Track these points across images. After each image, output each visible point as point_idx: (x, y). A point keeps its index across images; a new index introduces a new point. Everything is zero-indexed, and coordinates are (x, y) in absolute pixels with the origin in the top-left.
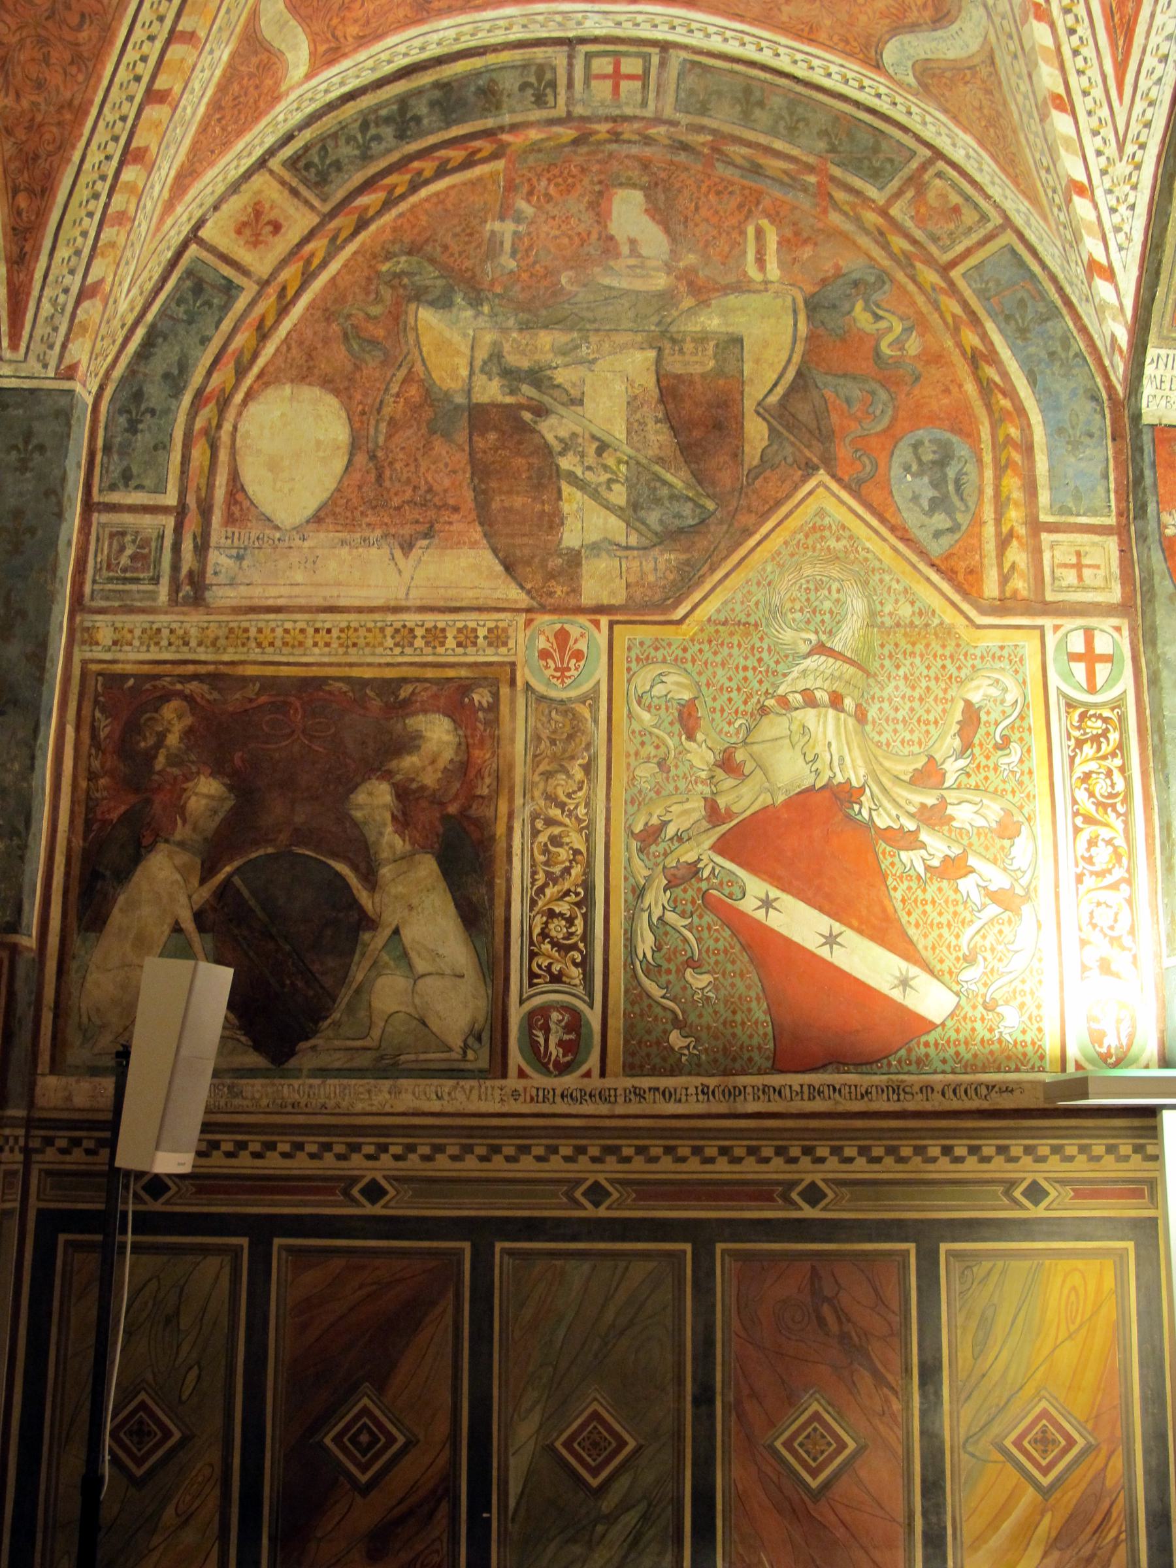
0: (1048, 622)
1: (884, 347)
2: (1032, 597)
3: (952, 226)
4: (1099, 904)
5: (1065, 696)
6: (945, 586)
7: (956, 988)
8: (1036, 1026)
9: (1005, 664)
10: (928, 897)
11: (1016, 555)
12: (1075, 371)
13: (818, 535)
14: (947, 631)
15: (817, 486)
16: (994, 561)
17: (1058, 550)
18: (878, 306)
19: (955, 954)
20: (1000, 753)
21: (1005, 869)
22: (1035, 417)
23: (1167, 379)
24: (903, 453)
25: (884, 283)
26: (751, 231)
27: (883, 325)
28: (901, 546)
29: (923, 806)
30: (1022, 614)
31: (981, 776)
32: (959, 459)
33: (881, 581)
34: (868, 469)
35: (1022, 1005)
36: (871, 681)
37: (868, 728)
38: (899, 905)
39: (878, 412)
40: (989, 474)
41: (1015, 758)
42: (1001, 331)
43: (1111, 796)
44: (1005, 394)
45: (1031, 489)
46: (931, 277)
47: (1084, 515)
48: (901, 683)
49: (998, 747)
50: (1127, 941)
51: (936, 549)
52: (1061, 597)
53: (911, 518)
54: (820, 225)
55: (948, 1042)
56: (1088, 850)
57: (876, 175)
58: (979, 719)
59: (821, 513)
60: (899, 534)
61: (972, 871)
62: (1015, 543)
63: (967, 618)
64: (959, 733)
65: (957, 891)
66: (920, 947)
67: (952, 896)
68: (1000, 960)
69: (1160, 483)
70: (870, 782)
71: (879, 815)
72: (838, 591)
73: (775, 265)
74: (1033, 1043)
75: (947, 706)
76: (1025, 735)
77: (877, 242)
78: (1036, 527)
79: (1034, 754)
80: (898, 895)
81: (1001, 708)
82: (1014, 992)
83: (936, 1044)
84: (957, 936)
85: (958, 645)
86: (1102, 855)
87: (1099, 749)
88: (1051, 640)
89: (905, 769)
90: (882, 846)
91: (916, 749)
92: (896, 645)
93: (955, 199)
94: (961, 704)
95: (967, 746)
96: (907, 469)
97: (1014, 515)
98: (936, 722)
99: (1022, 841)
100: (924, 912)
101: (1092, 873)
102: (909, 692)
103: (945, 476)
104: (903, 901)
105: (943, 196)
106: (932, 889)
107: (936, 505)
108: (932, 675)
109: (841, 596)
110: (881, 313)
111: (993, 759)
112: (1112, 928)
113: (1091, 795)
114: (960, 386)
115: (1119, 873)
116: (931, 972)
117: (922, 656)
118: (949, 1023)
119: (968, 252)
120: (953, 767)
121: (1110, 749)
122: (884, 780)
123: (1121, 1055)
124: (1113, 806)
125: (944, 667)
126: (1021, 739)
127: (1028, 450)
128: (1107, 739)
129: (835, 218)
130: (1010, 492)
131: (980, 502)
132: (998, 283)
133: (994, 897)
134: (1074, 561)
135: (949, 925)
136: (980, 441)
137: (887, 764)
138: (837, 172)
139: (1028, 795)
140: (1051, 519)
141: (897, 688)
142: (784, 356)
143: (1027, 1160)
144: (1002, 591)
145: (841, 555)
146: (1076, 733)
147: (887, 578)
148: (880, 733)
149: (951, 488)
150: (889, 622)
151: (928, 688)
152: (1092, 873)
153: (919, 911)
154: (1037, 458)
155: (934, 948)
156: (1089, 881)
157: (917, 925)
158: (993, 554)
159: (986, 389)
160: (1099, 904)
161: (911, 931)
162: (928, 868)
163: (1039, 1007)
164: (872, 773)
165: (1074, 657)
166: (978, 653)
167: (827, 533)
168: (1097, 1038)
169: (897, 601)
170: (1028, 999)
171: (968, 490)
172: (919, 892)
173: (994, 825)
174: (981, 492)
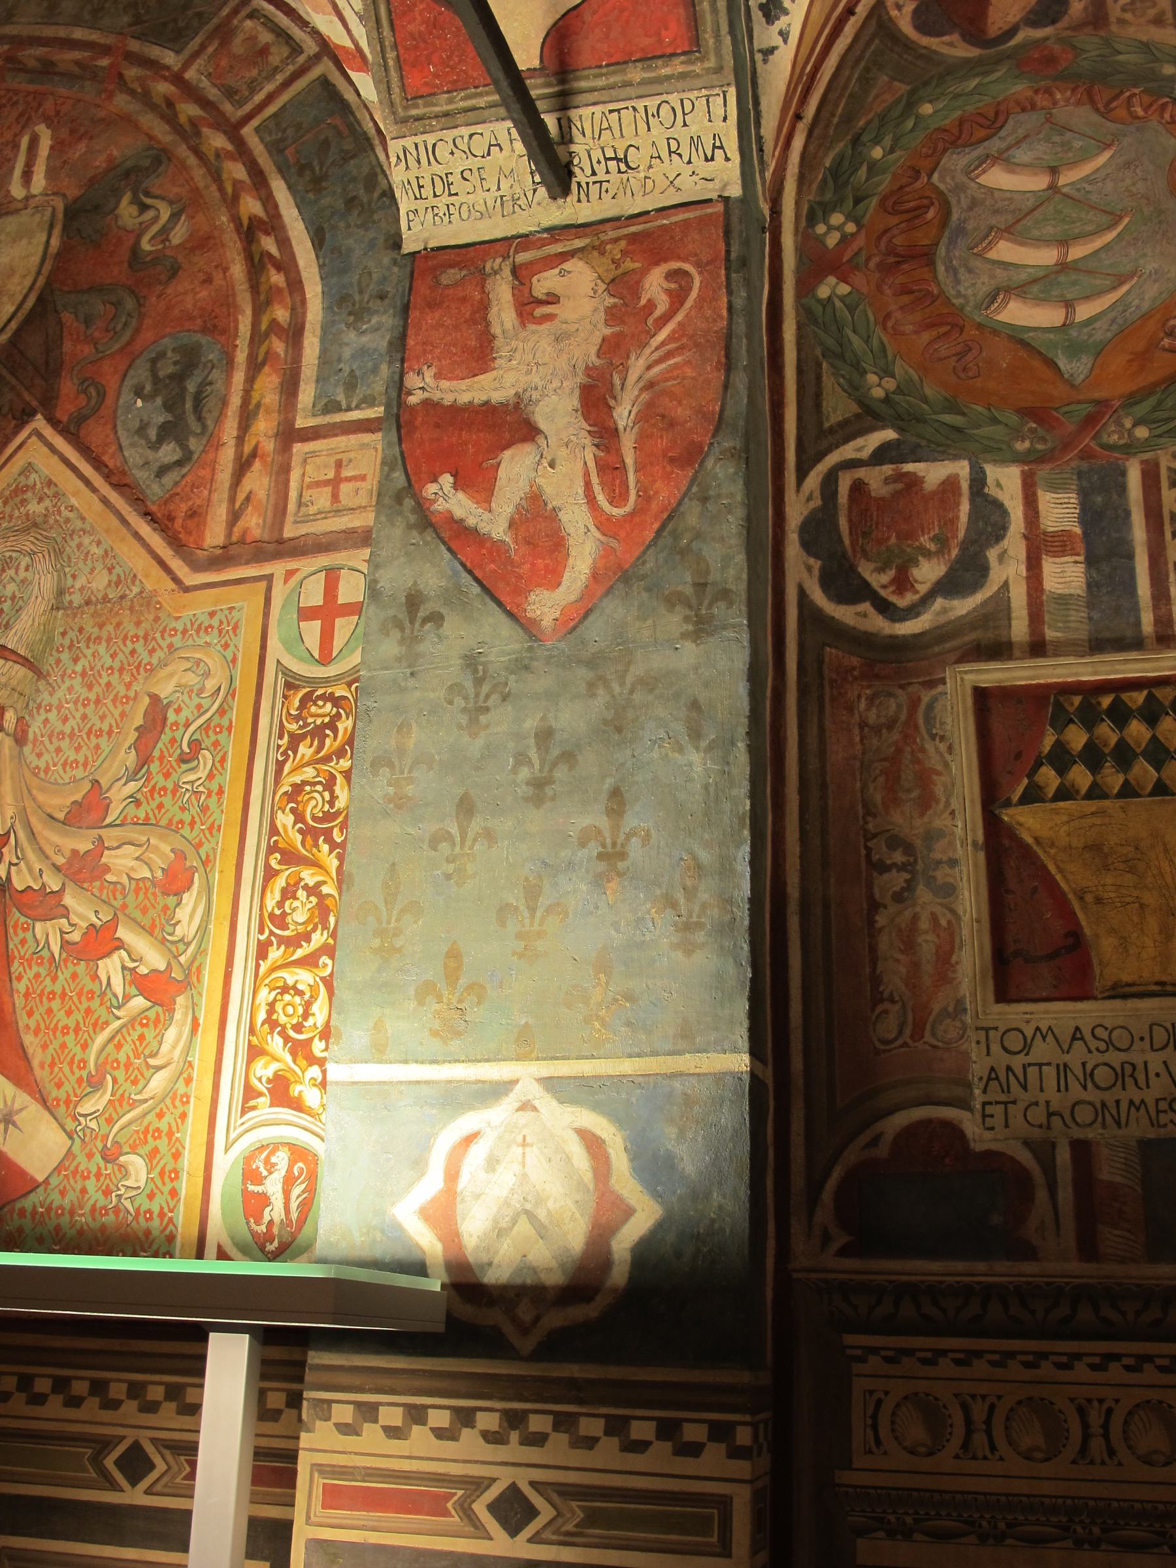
0: (277, 568)
1: (146, 246)
2: (266, 537)
3: (255, 72)
4: (285, 989)
5: (286, 672)
6: (156, 541)
7: (70, 1125)
8: (169, 1186)
9: (213, 638)
10: (58, 989)
11: (257, 482)
12: (376, 217)
13: (17, 500)
14: (148, 600)
15: (29, 437)
16: (226, 495)
17: (311, 462)
18: (147, 194)
19: (77, 1073)
20: (184, 767)
21: (164, 941)
22: (314, 290)
23: (426, 182)
24: (140, 373)
25: (160, 162)
26: (25, 141)
27: (150, 214)
28: (114, 497)
29: (75, 852)
30: (247, 563)
31: (154, 804)
32: (205, 365)
33: (79, 546)
34: (93, 402)
35: (156, 1151)
36: (41, 684)
37: (27, 749)
38: (19, 1002)
39: (119, 327)
40: (239, 377)
41: (203, 773)
42: (290, 188)
43: (328, 817)
44: (279, 268)
45: (290, 387)
46: (218, 141)
47: (357, 407)
48: (77, 682)
49: (183, 759)
50: (318, 1047)
51: (155, 490)
52: (303, 530)
53: (134, 455)
54: (102, 114)
55: (49, 1209)
56: (280, 904)
57: (175, 38)
58: (165, 719)
59: (29, 468)
60: (114, 479)
61: (120, 945)
62: (257, 465)
63: (176, 580)
64: (136, 745)
65: (95, 977)
66: (35, 1063)
67: (89, 985)
68: (135, 1082)
69: (411, 332)
70: (18, 827)
71: (19, 872)
72: (27, 569)
73: (42, 175)
74: (162, 1214)
75: (127, 708)
76: (222, 738)
77: (163, 117)
78: (289, 435)
79: (228, 764)
80: (21, 987)
81: (196, 701)
82: (146, 1132)
83: (34, 1212)
84: (85, 1047)
85: (157, 619)
86: (300, 911)
87: (321, 746)
88: (279, 592)
89: (59, 804)
90: (15, 916)
91: (79, 773)
92: (81, 630)
93: (266, 37)
94: (147, 700)
95: (144, 761)
96: (138, 392)
97: (264, 427)
98: (110, 733)
99: (189, 898)
100: (49, 1011)
101: (282, 940)
102: (84, 693)
103: (184, 390)
104: (27, 995)
105: (252, 38)
106: (63, 976)
107: (168, 432)
108: (117, 665)
109: (29, 575)
110: (148, 201)
111: (174, 777)
112: (298, 1028)
113: (299, 817)
114: (226, 270)
115: (319, 938)
116: (44, 1102)
117: (109, 640)
118: (54, 1181)
119: (270, 98)
120: (119, 794)
121: (337, 744)
122: (34, 821)
123: (286, 1238)
124: (328, 834)
125: (133, 652)
126: (216, 744)
127: (295, 334)
128: (335, 731)
129: (122, 102)
130: (262, 396)
131: (219, 421)
132: (299, 126)
133: (144, 984)
134: (331, 475)
135: (77, 1030)
136: (236, 336)
137: (41, 798)
138: (134, 46)
139: (210, 829)
140: (311, 422)
141: (70, 689)
142: (27, 283)
143: (130, 1407)
144: (229, 534)
145: (39, 520)
146: (293, 727)
147: (86, 540)
148: (39, 755)
149: (189, 405)
150: (77, 599)
151: (108, 684)
152: (282, 940)
153: (42, 1010)
154: (306, 343)
155: (52, 1065)
156: (275, 954)
157: (37, 1032)
158: (227, 485)
159: (256, 264)
160: (285, 989)
161: (28, 1039)
162: (65, 944)
163: (177, 1156)
164: (23, 813)
165: (307, 614)
166: (179, 626)
167: (29, 495)
168: (255, 1204)
169: (93, 570)
170: (162, 1144)
171: (211, 403)
172: (48, 981)
173: (159, 874)
174: (225, 402)
